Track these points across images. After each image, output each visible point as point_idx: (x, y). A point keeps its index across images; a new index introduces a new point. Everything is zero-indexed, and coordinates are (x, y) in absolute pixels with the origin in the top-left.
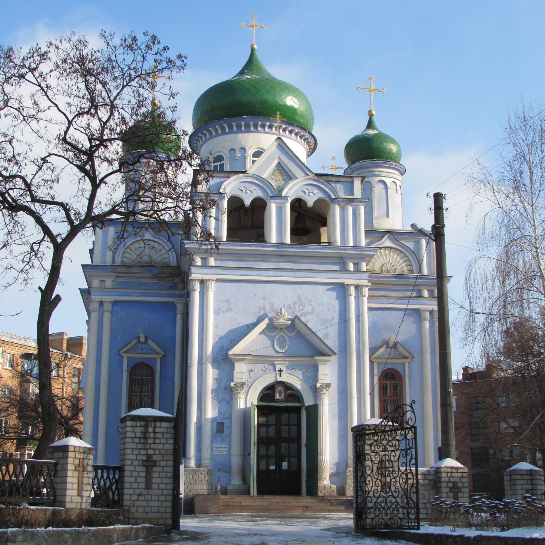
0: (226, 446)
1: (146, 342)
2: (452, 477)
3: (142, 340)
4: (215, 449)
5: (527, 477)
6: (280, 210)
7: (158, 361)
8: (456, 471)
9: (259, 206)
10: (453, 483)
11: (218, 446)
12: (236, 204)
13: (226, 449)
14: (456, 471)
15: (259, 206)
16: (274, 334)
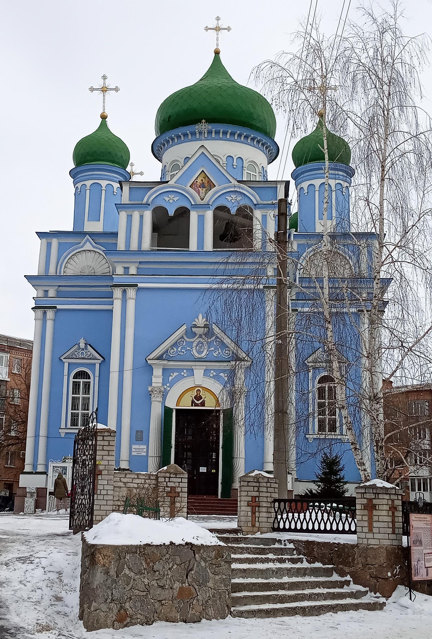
0: (145, 447)
1: (86, 348)
2: (169, 482)
3: (82, 345)
4: (133, 450)
5: (254, 484)
6: (201, 219)
7: (97, 366)
8: (174, 476)
9: (183, 213)
10: (171, 487)
11: (137, 447)
12: (159, 214)
13: (145, 450)
14: (174, 476)
15: (183, 213)
16: (192, 340)
